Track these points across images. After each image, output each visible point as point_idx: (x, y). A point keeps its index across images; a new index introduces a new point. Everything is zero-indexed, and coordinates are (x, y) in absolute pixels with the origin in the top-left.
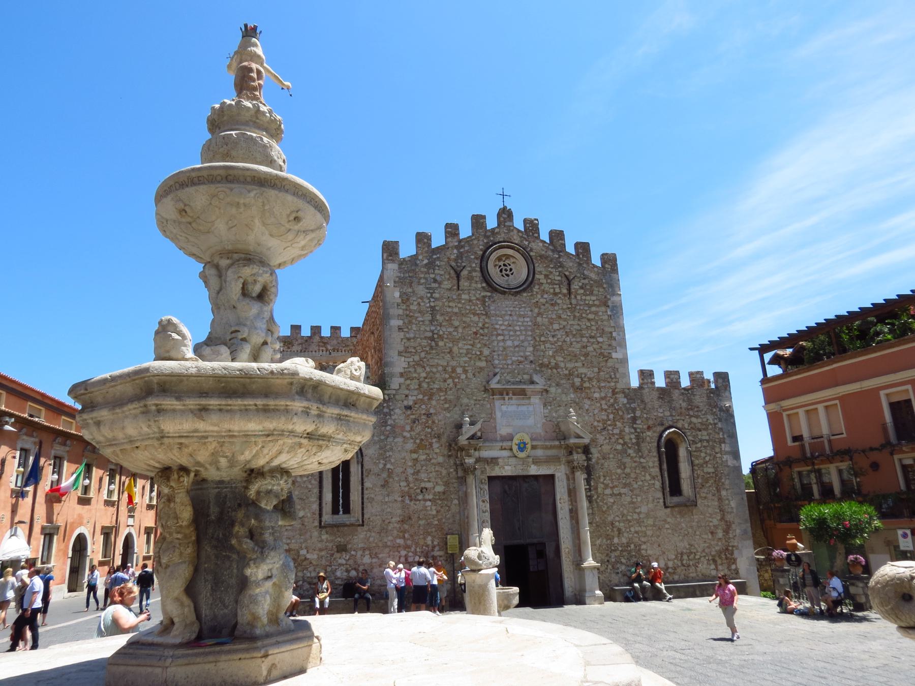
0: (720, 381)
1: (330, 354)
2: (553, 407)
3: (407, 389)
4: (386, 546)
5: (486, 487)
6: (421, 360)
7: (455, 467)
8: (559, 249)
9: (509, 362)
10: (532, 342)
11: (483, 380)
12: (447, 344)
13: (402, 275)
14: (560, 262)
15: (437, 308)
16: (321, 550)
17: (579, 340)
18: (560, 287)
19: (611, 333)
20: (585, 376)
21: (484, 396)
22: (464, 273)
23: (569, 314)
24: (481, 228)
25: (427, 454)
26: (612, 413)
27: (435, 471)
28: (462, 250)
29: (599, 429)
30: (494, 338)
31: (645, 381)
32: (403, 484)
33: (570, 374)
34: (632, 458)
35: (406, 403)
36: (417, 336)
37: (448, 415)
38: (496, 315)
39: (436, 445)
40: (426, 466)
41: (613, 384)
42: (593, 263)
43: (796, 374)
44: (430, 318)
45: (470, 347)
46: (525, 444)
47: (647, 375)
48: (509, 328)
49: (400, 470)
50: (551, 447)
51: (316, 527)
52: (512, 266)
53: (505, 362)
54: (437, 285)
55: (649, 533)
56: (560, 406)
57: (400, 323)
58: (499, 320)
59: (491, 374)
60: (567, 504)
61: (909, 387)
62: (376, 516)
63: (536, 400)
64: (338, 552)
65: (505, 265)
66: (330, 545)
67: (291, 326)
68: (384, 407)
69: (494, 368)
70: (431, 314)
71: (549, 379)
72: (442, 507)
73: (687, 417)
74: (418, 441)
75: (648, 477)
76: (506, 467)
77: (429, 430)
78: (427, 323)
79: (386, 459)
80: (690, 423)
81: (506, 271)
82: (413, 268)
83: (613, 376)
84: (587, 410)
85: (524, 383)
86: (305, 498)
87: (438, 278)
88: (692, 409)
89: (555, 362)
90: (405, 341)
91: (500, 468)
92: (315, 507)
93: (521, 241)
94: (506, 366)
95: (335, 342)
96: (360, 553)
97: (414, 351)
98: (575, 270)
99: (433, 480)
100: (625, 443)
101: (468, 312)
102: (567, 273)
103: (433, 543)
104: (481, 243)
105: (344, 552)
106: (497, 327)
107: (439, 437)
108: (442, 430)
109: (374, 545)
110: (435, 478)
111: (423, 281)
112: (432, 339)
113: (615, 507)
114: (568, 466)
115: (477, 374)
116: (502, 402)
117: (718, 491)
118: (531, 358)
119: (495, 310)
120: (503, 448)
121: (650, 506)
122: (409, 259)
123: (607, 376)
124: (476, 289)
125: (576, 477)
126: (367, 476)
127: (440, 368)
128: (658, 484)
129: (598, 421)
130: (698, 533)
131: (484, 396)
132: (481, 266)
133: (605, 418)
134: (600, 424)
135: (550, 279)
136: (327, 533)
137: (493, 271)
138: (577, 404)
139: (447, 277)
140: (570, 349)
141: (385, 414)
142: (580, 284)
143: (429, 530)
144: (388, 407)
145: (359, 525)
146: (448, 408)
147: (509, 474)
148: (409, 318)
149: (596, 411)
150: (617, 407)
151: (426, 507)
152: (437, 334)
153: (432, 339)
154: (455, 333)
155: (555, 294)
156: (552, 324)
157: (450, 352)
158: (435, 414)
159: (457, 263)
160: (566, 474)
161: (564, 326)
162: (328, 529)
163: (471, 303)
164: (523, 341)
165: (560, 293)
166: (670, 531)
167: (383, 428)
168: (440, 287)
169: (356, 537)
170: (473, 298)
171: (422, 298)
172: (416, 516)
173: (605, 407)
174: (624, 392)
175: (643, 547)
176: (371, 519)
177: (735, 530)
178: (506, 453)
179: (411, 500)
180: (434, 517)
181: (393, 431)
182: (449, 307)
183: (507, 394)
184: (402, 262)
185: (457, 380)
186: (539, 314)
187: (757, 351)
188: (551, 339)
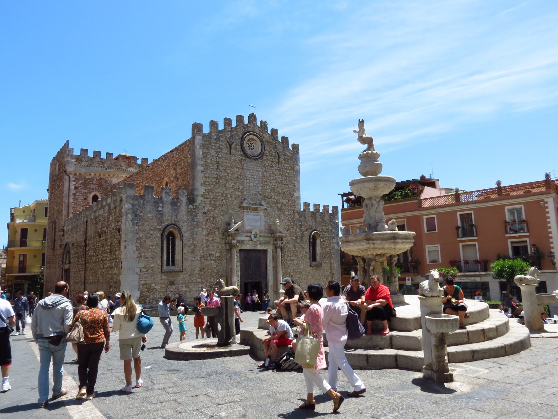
0: (335, 210)
1: (106, 169)
3: (204, 203)
4: (193, 282)
5: (239, 255)
8: (276, 139)
9: (251, 194)
13: (204, 143)
14: (275, 146)
15: (220, 162)
16: (162, 284)
17: (281, 185)
18: (275, 158)
19: (294, 183)
22: (233, 146)
24: (242, 123)
28: (232, 133)
29: (287, 229)
30: (245, 181)
32: (201, 251)
33: (277, 202)
34: (299, 243)
35: (203, 210)
36: (210, 176)
37: (223, 218)
38: (247, 169)
39: (217, 233)
40: (212, 243)
41: (294, 208)
43: (358, 208)
44: (216, 167)
45: (234, 184)
46: (257, 234)
47: (307, 205)
48: (252, 176)
49: (199, 245)
50: (267, 237)
51: (159, 272)
52: (254, 145)
53: (249, 193)
54: (220, 150)
55: (303, 278)
56: (271, 217)
57: (202, 168)
58: (247, 172)
59: (243, 199)
60: (272, 263)
61: (405, 219)
62: (188, 267)
63: (261, 213)
64: (170, 285)
65: (251, 144)
66: (166, 281)
67: (81, 149)
68: (193, 212)
71: (268, 204)
72: (218, 264)
74: (209, 230)
75: (304, 253)
76: (248, 245)
77: (214, 225)
78: (215, 170)
79: (194, 239)
80: (322, 229)
81: (251, 147)
82: (209, 139)
84: (283, 220)
85: (257, 205)
87: (221, 147)
88: (323, 222)
90: (204, 178)
92: (159, 262)
93: (260, 133)
94: (249, 196)
95: (109, 163)
96: (180, 285)
97: (208, 184)
98: (282, 150)
99: (215, 250)
100: (297, 237)
101: (234, 166)
102: (278, 152)
104: (242, 131)
106: (247, 175)
107: (218, 229)
108: (220, 226)
109: (187, 282)
111: (214, 147)
112: (217, 178)
114: (274, 246)
115: (237, 198)
116: (247, 213)
117: (331, 260)
118: (261, 193)
119: (246, 166)
121: (305, 265)
122: (207, 134)
123: (292, 204)
124: (238, 155)
125: (277, 251)
127: (220, 194)
128: (308, 256)
129: (287, 226)
133: (289, 224)
134: (287, 227)
136: (165, 275)
137: (246, 146)
138: (279, 216)
139: (225, 147)
141: (194, 216)
142: (283, 158)
144: (195, 212)
145: (180, 272)
146: (223, 214)
147: (249, 248)
148: (206, 166)
149: (286, 221)
153: (217, 178)
154: (228, 177)
156: (270, 176)
157: (225, 186)
158: (217, 217)
159: (230, 140)
160: (272, 250)
162: (165, 273)
164: (257, 184)
165: (275, 161)
166: (311, 277)
167: (193, 223)
168: (221, 152)
171: (213, 156)
172: (207, 267)
174: (298, 213)
175: (301, 284)
177: (335, 277)
178: (248, 239)
179: (205, 260)
180: (215, 268)
181: (197, 225)
182: (226, 162)
183: (250, 210)
184: (204, 136)
185: (227, 201)
186: (265, 171)
187: (341, 196)
188: (269, 184)
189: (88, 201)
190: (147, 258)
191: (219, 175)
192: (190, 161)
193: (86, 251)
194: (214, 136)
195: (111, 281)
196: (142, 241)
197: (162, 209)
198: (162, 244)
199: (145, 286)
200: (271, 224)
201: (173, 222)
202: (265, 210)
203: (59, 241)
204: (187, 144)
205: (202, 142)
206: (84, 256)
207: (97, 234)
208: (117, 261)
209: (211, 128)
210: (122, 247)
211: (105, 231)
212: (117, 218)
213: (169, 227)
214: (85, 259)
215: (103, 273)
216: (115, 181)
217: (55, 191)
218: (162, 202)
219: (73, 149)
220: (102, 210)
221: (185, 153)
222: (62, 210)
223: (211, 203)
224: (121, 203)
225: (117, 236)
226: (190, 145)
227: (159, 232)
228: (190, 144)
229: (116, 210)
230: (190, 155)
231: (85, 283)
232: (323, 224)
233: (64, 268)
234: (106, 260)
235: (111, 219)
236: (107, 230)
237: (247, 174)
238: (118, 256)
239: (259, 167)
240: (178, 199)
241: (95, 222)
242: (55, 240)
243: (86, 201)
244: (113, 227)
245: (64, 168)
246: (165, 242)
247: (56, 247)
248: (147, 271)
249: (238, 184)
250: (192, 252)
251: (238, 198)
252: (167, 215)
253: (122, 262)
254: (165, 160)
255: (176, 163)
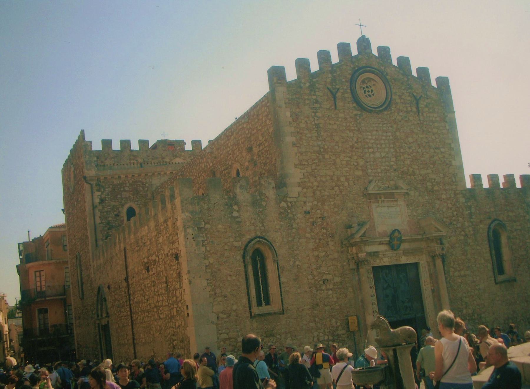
1: (141, 167)
2: (413, 207)
3: (305, 196)
5: (372, 276)
6: (313, 171)
7: (347, 261)
9: (379, 170)
10: (394, 153)
11: (361, 187)
12: (331, 157)
13: (291, 97)
15: (321, 126)
17: (427, 151)
18: (410, 106)
19: (450, 144)
20: (434, 181)
21: (363, 200)
22: (339, 95)
23: (419, 129)
25: (325, 251)
26: (455, 210)
27: (333, 266)
28: (335, 74)
29: (447, 223)
30: (366, 150)
31: (476, 183)
32: (310, 277)
35: (305, 208)
37: (338, 217)
39: (331, 244)
41: (454, 187)
42: (432, 85)
44: (316, 134)
45: (348, 159)
47: (476, 178)
48: (377, 142)
52: (373, 88)
53: (376, 171)
56: (418, 207)
62: (293, 305)
63: (401, 202)
64: (266, 337)
65: (367, 87)
69: (369, 176)
70: (317, 131)
73: (506, 211)
74: (317, 241)
75: (483, 261)
76: (385, 259)
77: (325, 231)
78: (314, 138)
83: (454, 180)
84: (438, 209)
86: (236, 294)
89: (412, 169)
90: (298, 155)
91: (380, 260)
92: (245, 301)
97: (306, 163)
100: (466, 235)
102: (415, 94)
103: (336, 324)
105: (271, 337)
106: (368, 141)
107: (333, 236)
108: (334, 230)
110: (334, 272)
111: (307, 102)
112: (319, 153)
113: (462, 285)
116: (377, 204)
118: (395, 167)
120: (382, 243)
122: (294, 82)
126: (282, 272)
127: (328, 178)
128: (490, 266)
129: (447, 218)
130: (518, 302)
131: (363, 200)
132: (351, 88)
135: (403, 99)
136: (257, 322)
137: (360, 92)
140: (422, 159)
142: (425, 103)
143: (333, 314)
145: (280, 314)
149: (444, 210)
150: (458, 206)
151: (329, 295)
152: (322, 148)
153: (319, 153)
154: (337, 147)
155: (408, 112)
157: (335, 163)
160: (427, 262)
161: (416, 139)
163: (346, 121)
165: (411, 111)
167: (290, 231)
169: (279, 324)
170: (348, 117)
171: (308, 117)
173: (450, 206)
174: (462, 194)
176: (289, 308)
179: (317, 291)
182: (330, 124)
183: (380, 198)
186: (398, 130)
188: (407, 150)
189: (122, 219)
190: (226, 297)
191: (322, 146)
192: (271, 130)
193: (129, 295)
194: (305, 84)
195: (174, 338)
196: (214, 269)
197: (238, 215)
198: (246, 272)
199: (228, 342)
200: (419, 218)
201: (259, 234)
202: (407, 196)
203: (89, 285)
204: (264, 103)
205: (288, 96)
206: (128, 303)
207: (142, 267)
208: (180, 305)
209: (298, 71)
210: (185, 282)
211: (155, 261)
212: (171, 238)
213: (253, 242)
214: (130, 308)
215: (160, 326)
216: (156, 182)
217: (73, 210)
218: (236, 203)
219: (91, 142)
220: (146, 227)
221: (262, 119)
222: (87, 237)
223: (315, 195)
224: (173, 213)
225: (174, 265)
226: (269, 104)
227: (239, 252)
228: (268, 102)
229: (167, 224)
230: (270, 120)
231: (134, 345)
232: (508, 208)
233: (100, 325)
234: (162, 306)
235: (161, 240)
236: (157, 259)
237: (367, 139)
238: (180, 298)
239: (386, 123)
240: (261, 194)
241: (137, 248)
242: (82, 283)
243: (118, 218)
244: (166, 252)
245: (81, 173)
246: (250, 268)
247: (85, 293)
248: (228, 317)
249: (355, 158)
250: (295, 280)
251: (358, 180)
252: (248, 223)
253: (187, 306)
254: (231, 136)
255: (250, 137)
